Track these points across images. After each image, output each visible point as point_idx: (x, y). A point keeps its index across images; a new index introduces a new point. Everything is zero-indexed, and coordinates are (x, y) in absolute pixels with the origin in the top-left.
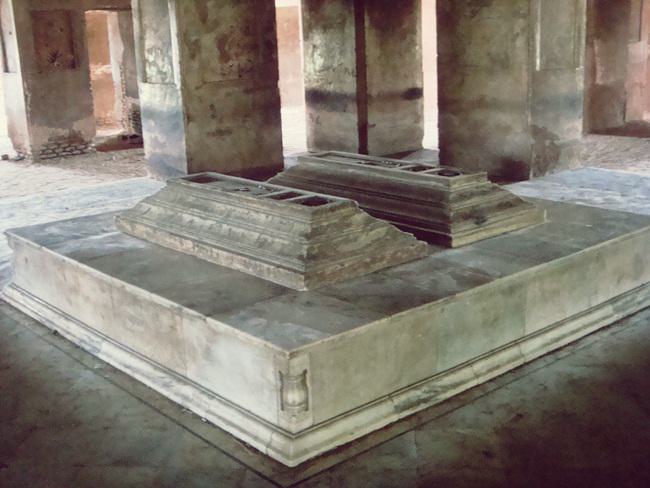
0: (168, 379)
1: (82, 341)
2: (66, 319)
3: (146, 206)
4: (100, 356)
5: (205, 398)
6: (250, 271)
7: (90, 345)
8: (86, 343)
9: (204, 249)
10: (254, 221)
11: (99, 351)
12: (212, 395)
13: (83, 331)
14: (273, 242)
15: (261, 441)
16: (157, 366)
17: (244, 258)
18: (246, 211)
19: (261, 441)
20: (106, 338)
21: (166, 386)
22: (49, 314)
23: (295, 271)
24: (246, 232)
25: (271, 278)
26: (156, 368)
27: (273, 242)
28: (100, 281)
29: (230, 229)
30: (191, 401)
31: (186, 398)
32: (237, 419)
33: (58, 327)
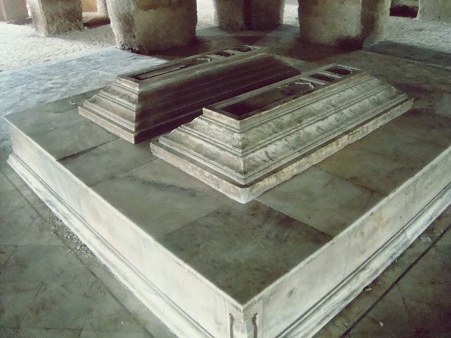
1: (391, 257)
2: (363, 269)
7: (399, 250)
8: (394, 254)
10: (351, 97)
11: (408, 240)
14: (378, 98)
18: (337, 95)
20: (403, 230)
22: (344, 293)
23: (401, 103)
24: (360, 104)
25: (400, 114)
26: (441, 197)
27: (378, 98)
29: (351, 111)
33: (363, 284)
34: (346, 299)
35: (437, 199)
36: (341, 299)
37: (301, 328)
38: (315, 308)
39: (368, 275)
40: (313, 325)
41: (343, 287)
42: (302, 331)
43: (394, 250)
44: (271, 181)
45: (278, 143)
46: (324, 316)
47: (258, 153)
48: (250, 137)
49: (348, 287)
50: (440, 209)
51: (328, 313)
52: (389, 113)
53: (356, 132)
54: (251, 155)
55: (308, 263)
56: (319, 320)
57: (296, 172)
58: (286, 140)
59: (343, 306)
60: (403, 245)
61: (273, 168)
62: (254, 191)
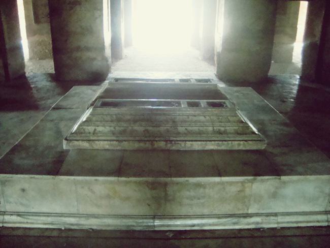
0: (235, 220)
3: (81, 127)
4: (156, 229)
5: (272, 218)
6: (223, 148)
8: (134, 226)
9: (178, 143)
12: (276, 215)
13: (124, 220)
15: (323, 221)
16: (219, 217)
17: (217, 142)
19: (323, 221)
21: (234, 224)
22: (72, 220)
26: (219, 218)
28: (135, 182)
29: (186, 129)
30: (262, 223)
31: (258, 223)
32: (301, 218)
34: (72, 225)
35: (214, 217)
36: (68, 222)
37: (31, 217)
38: (48, 215)
39: (98, 223)
40: (39, 222)
41: (74, 217)
42: (31, 219)
43: (135, 224)
44: (85, 145)
45: (107, 127)
46: (50, 222)
47: (89, 127)
48: (94, 119)
49: (77, 219)
50: (210, 225)
51: (54, 223)
52: (226, 143)
53: (178, 143)
54: (85, 127)
55: (31, 178)
56: (46, 222)
57: (107, 147)
58: (115, 128)
59: (68, 227)
60: (145, 226)
61: (92, 138)
62: (71, 144)
